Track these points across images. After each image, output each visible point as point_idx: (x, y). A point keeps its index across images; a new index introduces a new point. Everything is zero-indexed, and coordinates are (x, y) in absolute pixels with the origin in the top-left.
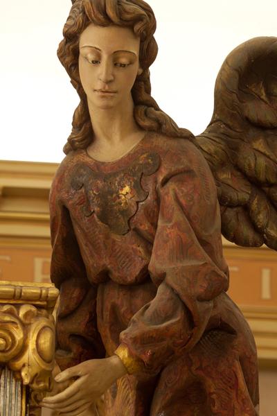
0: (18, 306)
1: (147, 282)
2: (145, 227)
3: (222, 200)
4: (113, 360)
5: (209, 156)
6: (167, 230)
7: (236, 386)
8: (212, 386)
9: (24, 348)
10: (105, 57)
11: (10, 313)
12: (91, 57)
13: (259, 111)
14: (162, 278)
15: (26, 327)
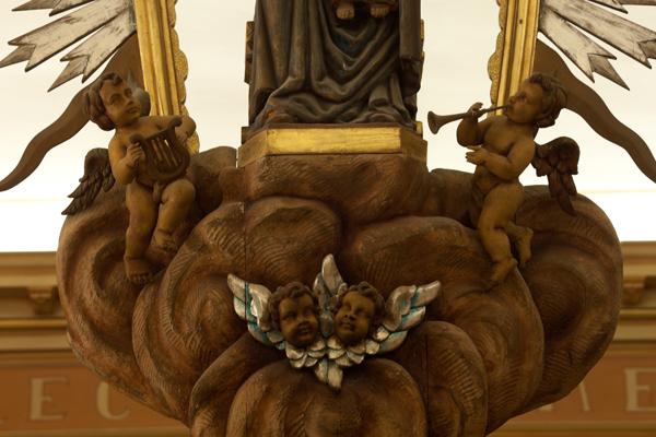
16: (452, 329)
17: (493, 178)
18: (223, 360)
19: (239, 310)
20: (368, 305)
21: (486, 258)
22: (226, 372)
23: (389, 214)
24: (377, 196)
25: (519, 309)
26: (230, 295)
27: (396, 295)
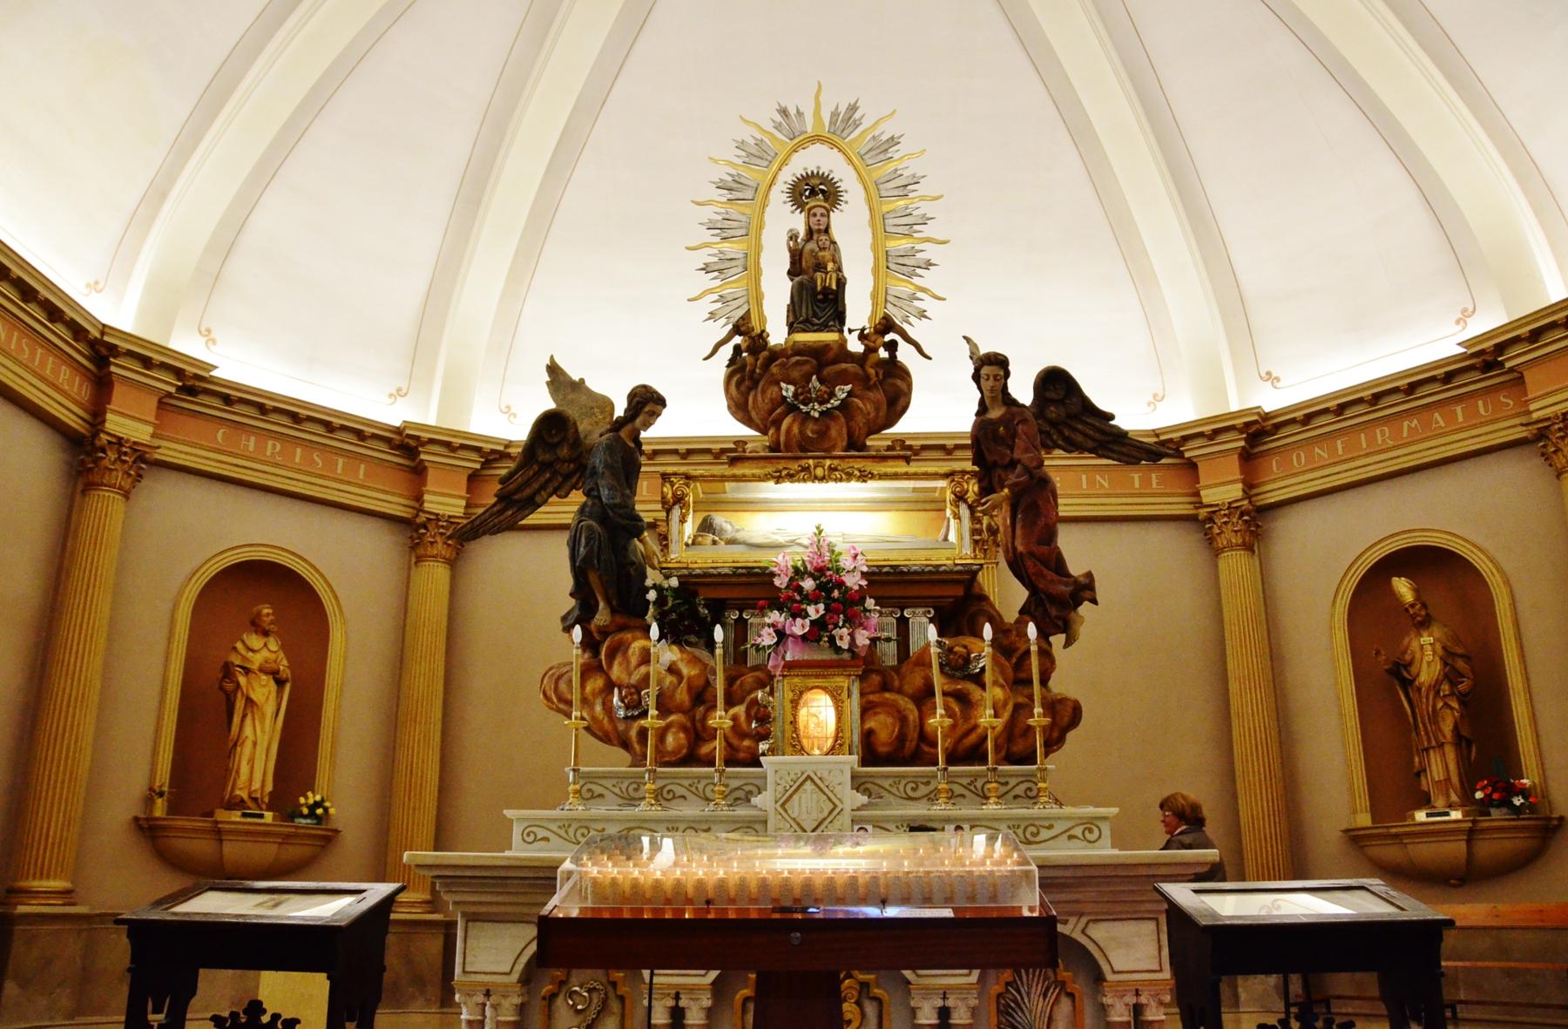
1: (1013, 464)
2: (1010, 443)
4: (1003, 494)
5: (1033, 414)
6: (1020, 443)
7: (1049, 502)
8: (1040, 503)
9: (967, 491)
10: (991, 378)
13: (1051, 395)
14: (1019, 461)
16: (856, 400)
17: (871, 350)
18: (779, 411)
19: (784, 393)
21: (867, 377)
23: (835, 361)
24: (831, 355)
25: (878, 395)
26: (781, 389)
27: (837, 388)
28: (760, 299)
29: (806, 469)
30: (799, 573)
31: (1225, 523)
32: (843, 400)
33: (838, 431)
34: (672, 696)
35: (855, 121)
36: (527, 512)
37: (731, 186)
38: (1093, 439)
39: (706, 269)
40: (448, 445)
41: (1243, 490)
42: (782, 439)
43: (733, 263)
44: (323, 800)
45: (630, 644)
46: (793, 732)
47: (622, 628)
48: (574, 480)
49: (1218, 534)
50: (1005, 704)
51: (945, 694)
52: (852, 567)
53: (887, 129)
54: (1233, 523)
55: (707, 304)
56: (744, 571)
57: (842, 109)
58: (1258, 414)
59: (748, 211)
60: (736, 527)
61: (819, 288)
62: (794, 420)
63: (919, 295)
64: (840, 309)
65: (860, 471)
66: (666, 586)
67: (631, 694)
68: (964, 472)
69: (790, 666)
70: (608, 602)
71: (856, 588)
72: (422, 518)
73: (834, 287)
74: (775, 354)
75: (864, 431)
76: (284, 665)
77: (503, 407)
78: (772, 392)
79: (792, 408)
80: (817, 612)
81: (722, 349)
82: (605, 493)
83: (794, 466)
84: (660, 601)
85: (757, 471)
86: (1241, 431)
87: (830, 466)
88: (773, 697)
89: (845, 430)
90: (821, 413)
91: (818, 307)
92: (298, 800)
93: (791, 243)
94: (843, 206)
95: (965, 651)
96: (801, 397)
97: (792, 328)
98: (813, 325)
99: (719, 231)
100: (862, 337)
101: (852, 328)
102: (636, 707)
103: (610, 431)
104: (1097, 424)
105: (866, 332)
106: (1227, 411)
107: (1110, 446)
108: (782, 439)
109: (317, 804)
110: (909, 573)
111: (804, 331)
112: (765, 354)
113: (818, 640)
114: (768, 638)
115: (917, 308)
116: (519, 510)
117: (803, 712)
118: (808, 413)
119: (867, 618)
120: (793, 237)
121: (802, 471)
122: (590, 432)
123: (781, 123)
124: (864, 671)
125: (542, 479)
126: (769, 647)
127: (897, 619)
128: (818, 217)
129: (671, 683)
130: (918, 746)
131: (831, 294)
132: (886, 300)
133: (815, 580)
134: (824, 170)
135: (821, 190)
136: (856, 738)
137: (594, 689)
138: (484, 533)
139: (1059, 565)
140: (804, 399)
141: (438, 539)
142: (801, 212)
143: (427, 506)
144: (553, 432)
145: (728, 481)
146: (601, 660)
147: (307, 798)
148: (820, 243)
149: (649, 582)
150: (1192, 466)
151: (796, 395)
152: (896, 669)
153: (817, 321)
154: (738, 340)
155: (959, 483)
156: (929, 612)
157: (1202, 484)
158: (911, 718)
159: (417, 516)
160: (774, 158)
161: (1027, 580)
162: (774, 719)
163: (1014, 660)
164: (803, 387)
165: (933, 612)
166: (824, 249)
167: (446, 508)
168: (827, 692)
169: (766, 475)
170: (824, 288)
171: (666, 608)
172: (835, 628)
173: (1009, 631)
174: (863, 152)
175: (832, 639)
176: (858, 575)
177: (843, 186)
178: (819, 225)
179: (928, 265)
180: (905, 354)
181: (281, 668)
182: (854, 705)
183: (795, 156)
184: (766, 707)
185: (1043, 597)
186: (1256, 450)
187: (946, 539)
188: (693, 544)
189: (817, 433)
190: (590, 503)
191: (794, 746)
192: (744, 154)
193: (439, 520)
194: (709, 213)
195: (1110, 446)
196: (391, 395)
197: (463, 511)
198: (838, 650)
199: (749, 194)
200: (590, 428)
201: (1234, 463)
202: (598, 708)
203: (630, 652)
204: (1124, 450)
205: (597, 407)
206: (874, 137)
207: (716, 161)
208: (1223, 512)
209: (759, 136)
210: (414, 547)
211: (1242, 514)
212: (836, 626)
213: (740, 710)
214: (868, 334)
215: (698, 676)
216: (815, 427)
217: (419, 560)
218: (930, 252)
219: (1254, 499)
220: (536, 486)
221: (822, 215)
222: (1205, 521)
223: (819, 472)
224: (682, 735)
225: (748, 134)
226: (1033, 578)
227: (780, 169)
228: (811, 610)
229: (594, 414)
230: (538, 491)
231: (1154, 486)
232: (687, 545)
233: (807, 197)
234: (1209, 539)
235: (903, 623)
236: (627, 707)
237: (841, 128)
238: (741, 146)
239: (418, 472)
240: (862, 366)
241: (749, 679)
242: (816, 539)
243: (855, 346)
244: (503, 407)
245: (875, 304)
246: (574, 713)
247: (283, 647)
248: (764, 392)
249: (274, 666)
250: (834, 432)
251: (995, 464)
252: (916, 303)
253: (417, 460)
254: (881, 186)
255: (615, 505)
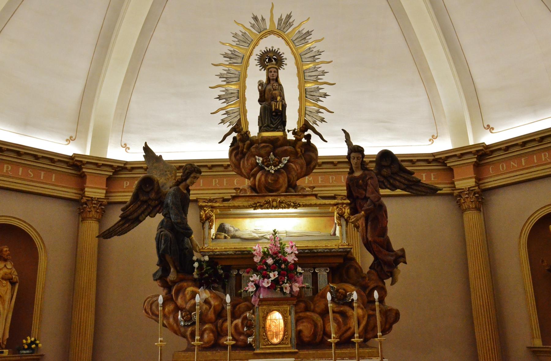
0: (343, 205)
1: (366, 198)
2: (365, 188)
3: (379, 181)
4: (361, 214)
6: (369, 189)
7: (384, 216)
9: (345, 212)
11: (341, 206)
12: (353, 158)
13: (384, 163)
14: (369, 198)
15: (345, 209)
16: (292, 164)
17: (298, 140)
18: (255, 169)
19: (258, 161)
20: (278, 160)
21: (297, 153)
22: (255, 171)
23: (282, 145)
24: (279, 143)
25: (302, 161)
26: (256, 159)
27: (283, 159)
28: (245, 112)
29: (268, 203)
30: (266, 255)
31: (467, 198)
32: (285, 164)
33: (283, 180)
34: (206, 315)
35: (290, 23)
36: (135, 225)
37: (231, 56)
38: (404, 184)
39: (220, 98)
40: (96, 164)
41: (476, 182)
42: (257, 183)
43: (233, 95)
44: (35, 340)
45: (186, 288)
46: (264, 332)
47: (182, 280)
48: (158, 209)
49: (464, 203)
50: (364, 317)
51: (334, 312)
52: (291, 252)
53: (306, 28)
54: (471, 198)
55: (220, 116)
56: (239, 253)
57: (284, 17)
58: (483, 146)
59: (239, 69)
60: (236, 228)
61: (273, 110)
62: (262, 174)
63: (321, 110)
64: (284, 120)
65: (294, 203)
66: (203, 260)
67: (187, 315)
68: (343, 204)
69: (261, 300)
70: (175, 268)
71: (293, 262)
72: (84, 200)
73: (281, 109)
74: (253, 142)
75: (296, 178)
76: (15, 276)
77: (123, 145)
78: (252, 160)
79: (261, 168)
80: (274, 276)
81: (228, 137)
82: (172, 216)
83: (262, 200)
84: (200, 268)
85: (246, 204)
86: (474, 154)
87: (280, 201)
88: (254, 315)
89: (286, 180)
90: (275, 171)
91: (273, 118)
92: (23, 341)
93: (260, 87)
94: (285, 67)
95: (344, 291)
96: (266, 164)
97: (261, 130)
98: (271, 128)
99: (225, 79)
100: (294, 133)
101: (289, 129)
102: (189, 319)
103: (175, 185)
104: (406, 177)
105: (296, 131)
106: (468, 145)
107: (412, 187)
108: (257, 183)
109: (32, 343)
110: (317, 252)
111: (267, 131)
112: (248, 142)
113: (275, 289)
114: (251, 288)
115: (320, 117)
116: (132, 223)
117: (268, 322)
118: (269, 171)
119: (298, 277)
120: (261, 84)
121: (266, 204)
122: (165, 184)
123: (254, 24)
124: (296, 302)
125: (142, 209)
126: (252, 292)
127: (312, 273)
128: (273, 73)
129: (206, 308)
130: (323, 337)
131: (279, 112)
132: (305, 114)
133: (273, 259)
134: (275, 48)
135: (274, 59)
136: (294, 335)
137: (169, 310)
138: (115, 235)
139: (388, 246)
140: (267, 165)
141: (92, 209)
142: (264, 70)
143: (87, 194)
144: (147, 186)
145: (231, 208)
146: (172, 295)
147: (27, 340)
148: (274, 87)
149: (195, 258)
150: (451, 170)
151: (263, 162)
152: (312, 299)
153: (273, 126)
154: (234, 134)
155: (341, 209)
156: (327, 270)
157: (455, 179)
158: (319, 324)
159: (82, 198)
160: (251, 42)
161: (372, 252)
162: (255, 326)
163: (367, 292)
164: (266, 159)
165: (329, 269)
166: (276, 89)
167: (96, 194)
168: (279, 313)
169: (249, 206)
170: (276, 109)
171: (203, 271)
172: (283, 284)
173: (365, 277)
174: (294, 39)
175: (282, 289)
176: (293, 255)
177: (284, 56)
178: (273, 76)
179: (325, 95)
180: (315, 140)
181: (14, 276)
182: (292, 318)
183: (261, 41)
184: (251, 320)
185: (381, 262)
186: (483, 162)
187: (334, 234)
188: (215, 238)
189: (273, 181)
190: (166, 220)
191: (264, 339)
192: (236, 40)
193: (92, 200)
194: (220, 70)
195: (412, 187)
196: (67, 140)
197: (104, 195)
198: (284, 293)
199: (239, 60)
200: (165, 181)
201: (471, 168)
202: (171, 320)
203: (186, 292)
204: (419, 189)
205: (168, 171)
206: (299, 32)
207: (223, 44)
208: (465, 192)
209: (244, 31)
210: (80, 214)
211: (475, 194)
212: (283, 283)
213: (238, 321)
214: (297, 132)
215: (219, 305)
216: (273, 178)
217: (83, 219)
218: (326, 89)
219: (481, 185)
220: (139, 212)
221: (275, 72)
222: (457, 196)
223: (275, 204)
224: (211, 334)
225: (238, 30)
226: (376, 253)
227: (254, 48)
228: (271, 275)
229: (167, 175)
230: (141, 214)
231: (433, 179)
232: (212, 239)
233: (267, 63)
234: (459, 204)
235: (315, 275)
236: (185, 321)
237: (284, 27)
238: (235, 35)
239: (82, 177)
240: (294, 147)
241: (243, 305)
242: (273, 237)
243: (290, 137)
244: (123, 145)
245: (300, 115)
246: (160, 339)
247: (14, 266)
248: (248, 160)
249: (10, 276)
250: (281, 180)
251: (358, 197)
252: (320, 114)
253: (81, 172)
254: (302, 57)
255: (178, 223)
